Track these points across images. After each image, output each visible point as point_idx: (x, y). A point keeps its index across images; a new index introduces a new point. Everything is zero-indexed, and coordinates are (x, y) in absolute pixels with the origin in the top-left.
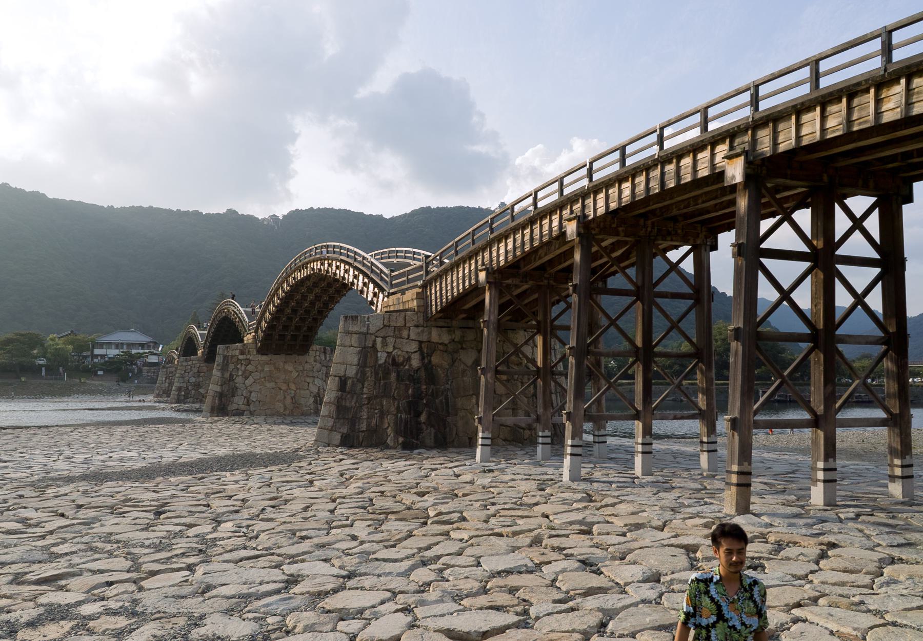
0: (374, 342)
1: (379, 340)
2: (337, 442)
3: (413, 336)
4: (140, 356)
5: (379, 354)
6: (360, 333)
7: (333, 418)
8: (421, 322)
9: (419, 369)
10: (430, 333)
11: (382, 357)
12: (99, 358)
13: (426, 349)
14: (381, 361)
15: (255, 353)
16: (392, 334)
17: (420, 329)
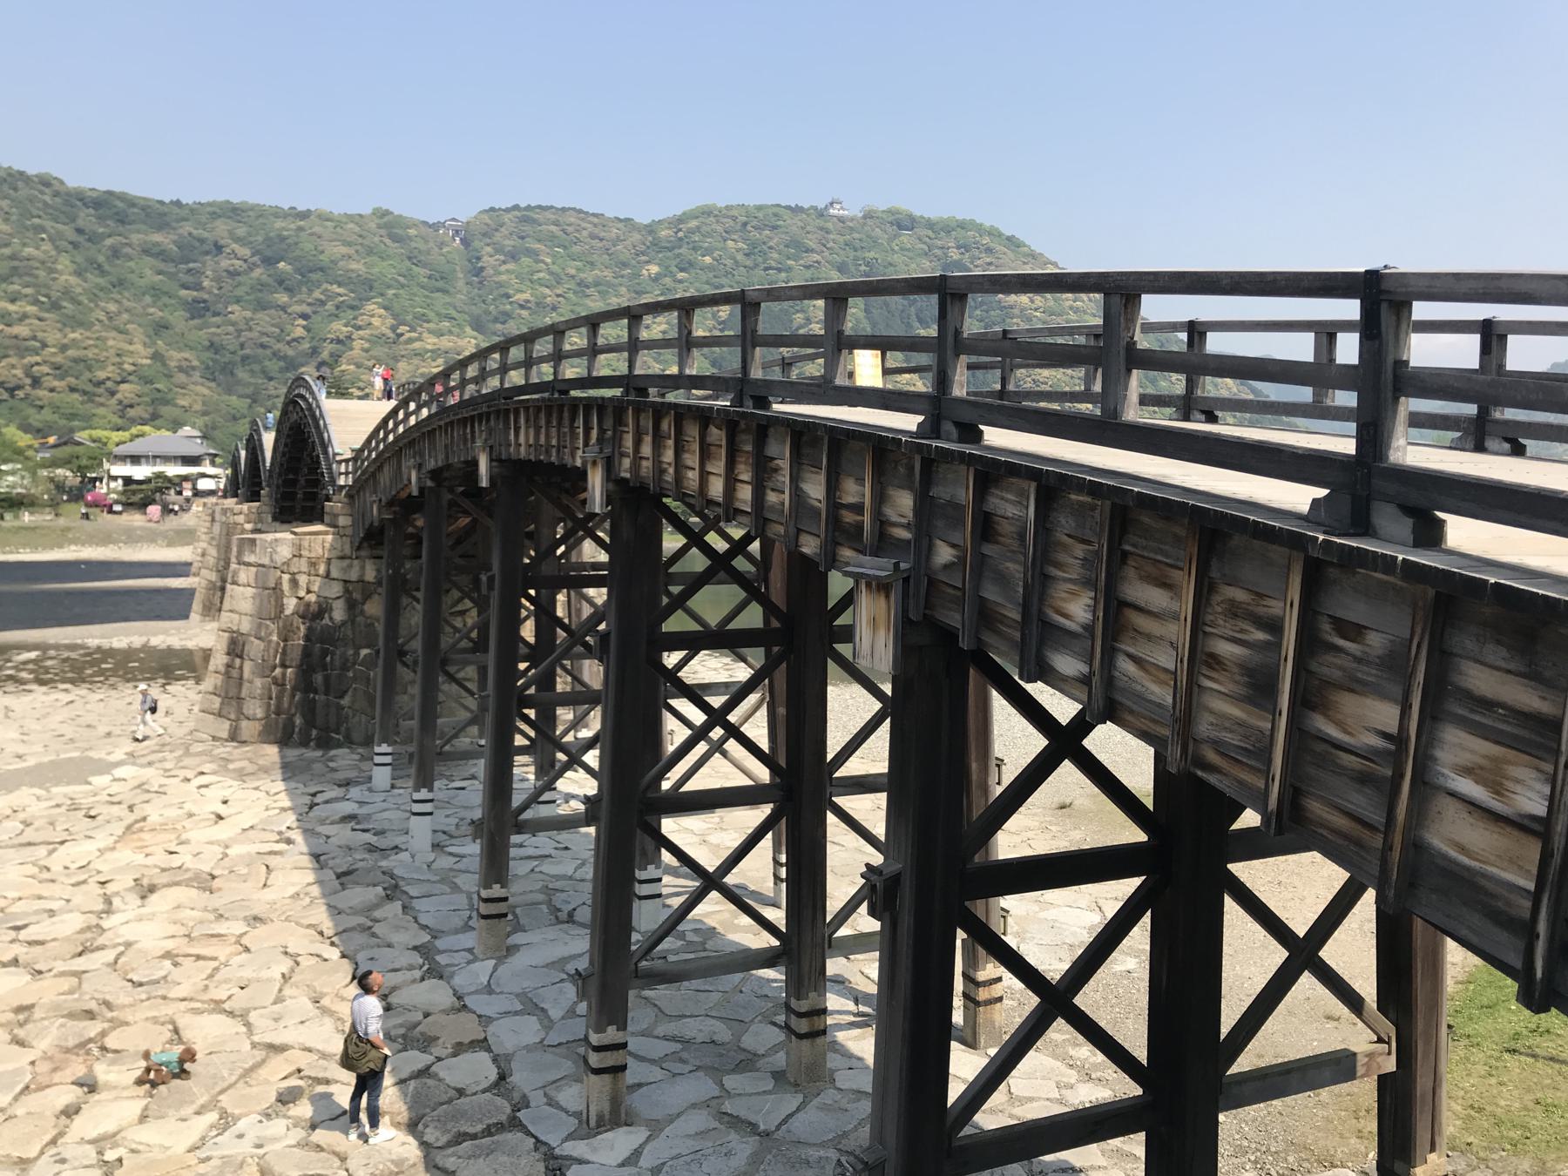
0: (279, 583)
1: (286, 577)
2: (225, 735)
3: (334, 574)
4: (185, 478)
5: (285, 601)
6: (260, 565)
7: (219, 696)
8: (348, 551)
9: (344, 623)
10: (363, 568)
11: (291, 604)
12: (120, 481)
13: (355, 594)
14: (288, 612)
15: (270, 519)
16: (304, 568)
17: (347, 562)
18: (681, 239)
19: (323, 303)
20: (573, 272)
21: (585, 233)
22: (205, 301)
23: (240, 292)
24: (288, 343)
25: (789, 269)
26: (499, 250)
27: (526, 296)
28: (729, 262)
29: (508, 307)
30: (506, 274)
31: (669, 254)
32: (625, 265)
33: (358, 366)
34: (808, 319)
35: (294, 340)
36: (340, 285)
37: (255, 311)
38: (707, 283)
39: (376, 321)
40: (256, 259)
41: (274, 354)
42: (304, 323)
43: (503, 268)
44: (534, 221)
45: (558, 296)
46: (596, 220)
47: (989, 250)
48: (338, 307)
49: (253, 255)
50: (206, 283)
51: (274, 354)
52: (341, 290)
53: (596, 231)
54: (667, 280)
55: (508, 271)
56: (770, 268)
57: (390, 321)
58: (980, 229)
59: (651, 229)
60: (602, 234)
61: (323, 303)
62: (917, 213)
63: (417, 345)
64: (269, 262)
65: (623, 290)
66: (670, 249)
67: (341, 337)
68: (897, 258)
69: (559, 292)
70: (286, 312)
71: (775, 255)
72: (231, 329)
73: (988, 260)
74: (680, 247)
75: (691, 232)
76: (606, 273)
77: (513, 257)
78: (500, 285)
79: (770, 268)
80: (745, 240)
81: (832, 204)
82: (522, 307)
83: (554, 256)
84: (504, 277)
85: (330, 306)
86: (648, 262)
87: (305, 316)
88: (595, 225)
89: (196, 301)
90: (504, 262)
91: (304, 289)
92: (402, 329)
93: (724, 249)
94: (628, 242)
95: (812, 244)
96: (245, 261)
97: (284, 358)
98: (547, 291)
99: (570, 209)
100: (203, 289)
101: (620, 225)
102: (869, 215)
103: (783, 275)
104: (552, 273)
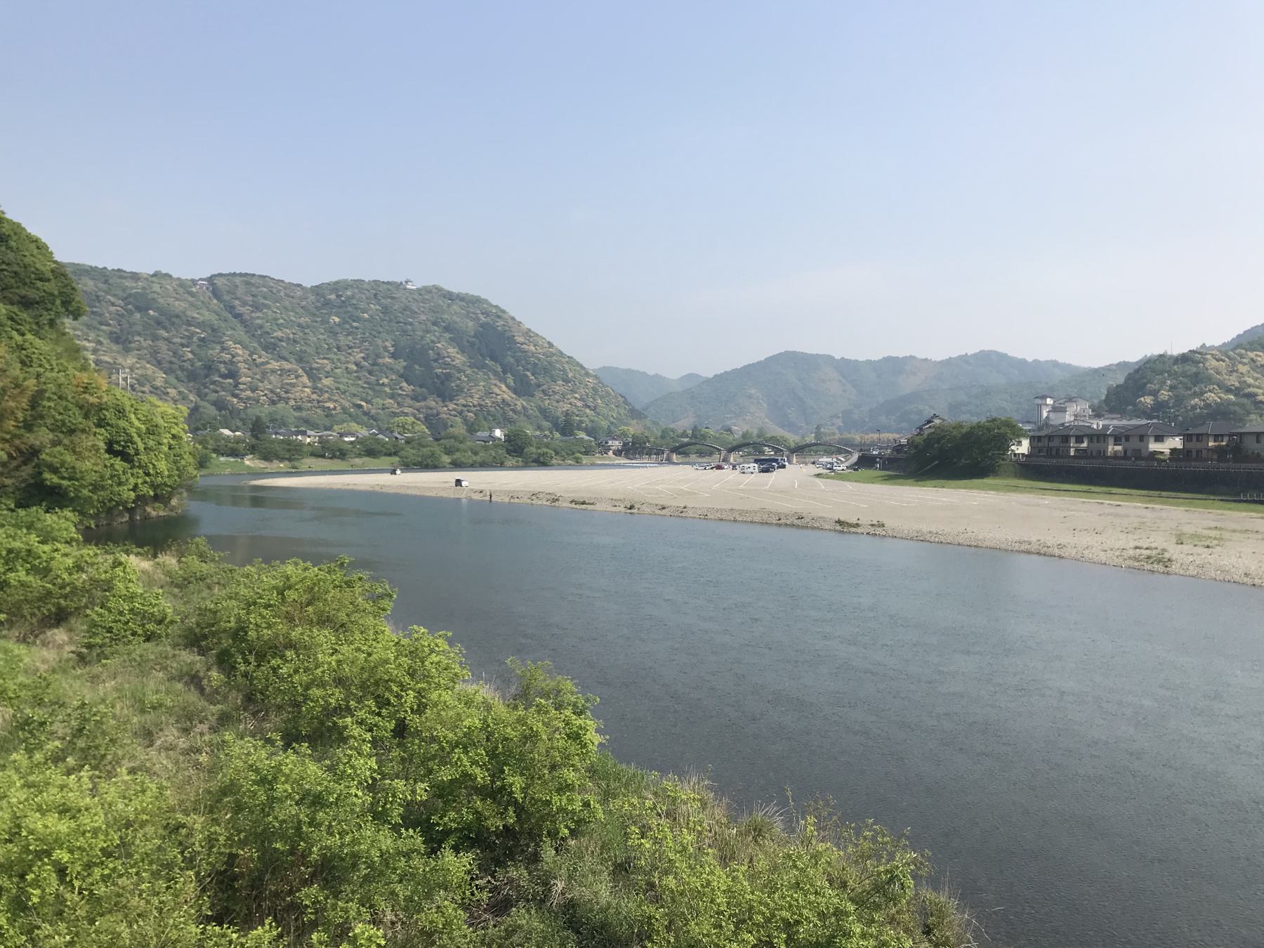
18: (343, 302)
19: (190, 338)
20: (294, 319)
21: (282, 294)
22: (115, 333)
23: (139, 328)
24: (184, 361)
25: (411, 324)
26: (244, 304)
27: (279, 334)
28: (378, 318)
29: (273, 340)
30: (258, 318)
31: (340, 310)
32: (314, 315)
33: (252, 378)
34: (438, 354)
35: (189, 360)
36: (196, 327)
37: (153, 341)
38: (373, 330)
39: (240, 352)
40: (130, 306)
41: (180, 367)
42: (189, 349)
43: (253, 315)
44: (253, 285)
45: (294, 334)
46: (284, 285)
47: (499, 317)
48: (202, 340)
49: (126, 305)
50: (111, 322)
51: (180, 367)
52: (198, 330)
53: (288, 292)
54: (347, 326)
55: (258, 318)
56: (400, 322)
57: (248, 352)
58: (486, 301)
59: (317, 290)
60: (292, 294)
61: (190, 338)
62: (451, 290)
63: (269, 366)
64: (139, 309)
65: (323, 331)
66: (340, 307)
67: (226, 360)
68: (455, 318)
69: (294, 331)
70: (170, 342)
71: (399, 315)
72: (146, 351)
73: (502, 323)
74: (346, 307)
75: (349, 298)
76: (307, 319)
77: (257, 308)
78: (261, 327)
79: (400, 322)
80: (379, 305)
81: (407, 282)
82: (281, 340)
83: (277, 308)
84: (259, 321)
85: (195, 339)
86: (330, 314)
87: (183, 345)
88: (285, 288)
89: (111, 333)
90: (252, 311)
91: (173, 329)
92: (255, 357)
93: (372, 309)
94: (308, 300)
95: (416, 310)
96: (122, 307)
97: (187, 370)
98: (288, 331)
99: (266, 276)
100: (109, 325)
101: (299, 289)
102: (428, 290)
103: (409, 327)
104: (285, 320)
